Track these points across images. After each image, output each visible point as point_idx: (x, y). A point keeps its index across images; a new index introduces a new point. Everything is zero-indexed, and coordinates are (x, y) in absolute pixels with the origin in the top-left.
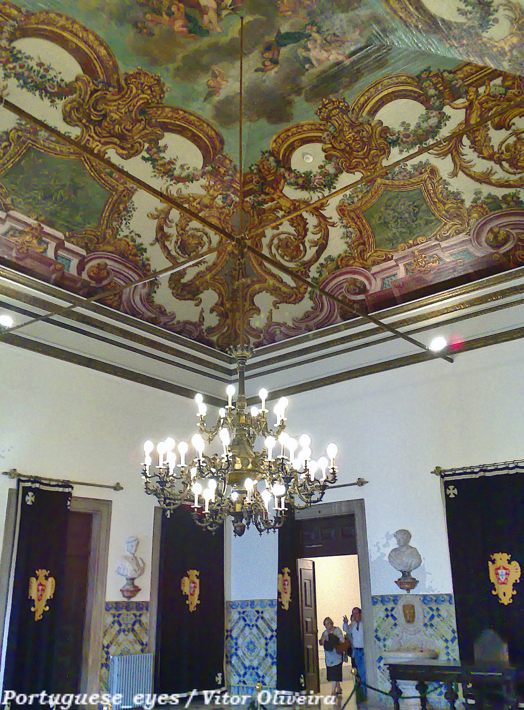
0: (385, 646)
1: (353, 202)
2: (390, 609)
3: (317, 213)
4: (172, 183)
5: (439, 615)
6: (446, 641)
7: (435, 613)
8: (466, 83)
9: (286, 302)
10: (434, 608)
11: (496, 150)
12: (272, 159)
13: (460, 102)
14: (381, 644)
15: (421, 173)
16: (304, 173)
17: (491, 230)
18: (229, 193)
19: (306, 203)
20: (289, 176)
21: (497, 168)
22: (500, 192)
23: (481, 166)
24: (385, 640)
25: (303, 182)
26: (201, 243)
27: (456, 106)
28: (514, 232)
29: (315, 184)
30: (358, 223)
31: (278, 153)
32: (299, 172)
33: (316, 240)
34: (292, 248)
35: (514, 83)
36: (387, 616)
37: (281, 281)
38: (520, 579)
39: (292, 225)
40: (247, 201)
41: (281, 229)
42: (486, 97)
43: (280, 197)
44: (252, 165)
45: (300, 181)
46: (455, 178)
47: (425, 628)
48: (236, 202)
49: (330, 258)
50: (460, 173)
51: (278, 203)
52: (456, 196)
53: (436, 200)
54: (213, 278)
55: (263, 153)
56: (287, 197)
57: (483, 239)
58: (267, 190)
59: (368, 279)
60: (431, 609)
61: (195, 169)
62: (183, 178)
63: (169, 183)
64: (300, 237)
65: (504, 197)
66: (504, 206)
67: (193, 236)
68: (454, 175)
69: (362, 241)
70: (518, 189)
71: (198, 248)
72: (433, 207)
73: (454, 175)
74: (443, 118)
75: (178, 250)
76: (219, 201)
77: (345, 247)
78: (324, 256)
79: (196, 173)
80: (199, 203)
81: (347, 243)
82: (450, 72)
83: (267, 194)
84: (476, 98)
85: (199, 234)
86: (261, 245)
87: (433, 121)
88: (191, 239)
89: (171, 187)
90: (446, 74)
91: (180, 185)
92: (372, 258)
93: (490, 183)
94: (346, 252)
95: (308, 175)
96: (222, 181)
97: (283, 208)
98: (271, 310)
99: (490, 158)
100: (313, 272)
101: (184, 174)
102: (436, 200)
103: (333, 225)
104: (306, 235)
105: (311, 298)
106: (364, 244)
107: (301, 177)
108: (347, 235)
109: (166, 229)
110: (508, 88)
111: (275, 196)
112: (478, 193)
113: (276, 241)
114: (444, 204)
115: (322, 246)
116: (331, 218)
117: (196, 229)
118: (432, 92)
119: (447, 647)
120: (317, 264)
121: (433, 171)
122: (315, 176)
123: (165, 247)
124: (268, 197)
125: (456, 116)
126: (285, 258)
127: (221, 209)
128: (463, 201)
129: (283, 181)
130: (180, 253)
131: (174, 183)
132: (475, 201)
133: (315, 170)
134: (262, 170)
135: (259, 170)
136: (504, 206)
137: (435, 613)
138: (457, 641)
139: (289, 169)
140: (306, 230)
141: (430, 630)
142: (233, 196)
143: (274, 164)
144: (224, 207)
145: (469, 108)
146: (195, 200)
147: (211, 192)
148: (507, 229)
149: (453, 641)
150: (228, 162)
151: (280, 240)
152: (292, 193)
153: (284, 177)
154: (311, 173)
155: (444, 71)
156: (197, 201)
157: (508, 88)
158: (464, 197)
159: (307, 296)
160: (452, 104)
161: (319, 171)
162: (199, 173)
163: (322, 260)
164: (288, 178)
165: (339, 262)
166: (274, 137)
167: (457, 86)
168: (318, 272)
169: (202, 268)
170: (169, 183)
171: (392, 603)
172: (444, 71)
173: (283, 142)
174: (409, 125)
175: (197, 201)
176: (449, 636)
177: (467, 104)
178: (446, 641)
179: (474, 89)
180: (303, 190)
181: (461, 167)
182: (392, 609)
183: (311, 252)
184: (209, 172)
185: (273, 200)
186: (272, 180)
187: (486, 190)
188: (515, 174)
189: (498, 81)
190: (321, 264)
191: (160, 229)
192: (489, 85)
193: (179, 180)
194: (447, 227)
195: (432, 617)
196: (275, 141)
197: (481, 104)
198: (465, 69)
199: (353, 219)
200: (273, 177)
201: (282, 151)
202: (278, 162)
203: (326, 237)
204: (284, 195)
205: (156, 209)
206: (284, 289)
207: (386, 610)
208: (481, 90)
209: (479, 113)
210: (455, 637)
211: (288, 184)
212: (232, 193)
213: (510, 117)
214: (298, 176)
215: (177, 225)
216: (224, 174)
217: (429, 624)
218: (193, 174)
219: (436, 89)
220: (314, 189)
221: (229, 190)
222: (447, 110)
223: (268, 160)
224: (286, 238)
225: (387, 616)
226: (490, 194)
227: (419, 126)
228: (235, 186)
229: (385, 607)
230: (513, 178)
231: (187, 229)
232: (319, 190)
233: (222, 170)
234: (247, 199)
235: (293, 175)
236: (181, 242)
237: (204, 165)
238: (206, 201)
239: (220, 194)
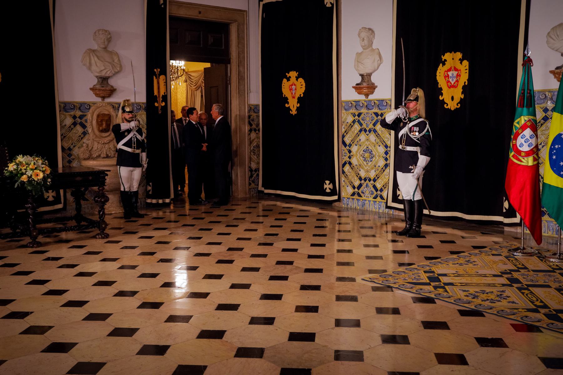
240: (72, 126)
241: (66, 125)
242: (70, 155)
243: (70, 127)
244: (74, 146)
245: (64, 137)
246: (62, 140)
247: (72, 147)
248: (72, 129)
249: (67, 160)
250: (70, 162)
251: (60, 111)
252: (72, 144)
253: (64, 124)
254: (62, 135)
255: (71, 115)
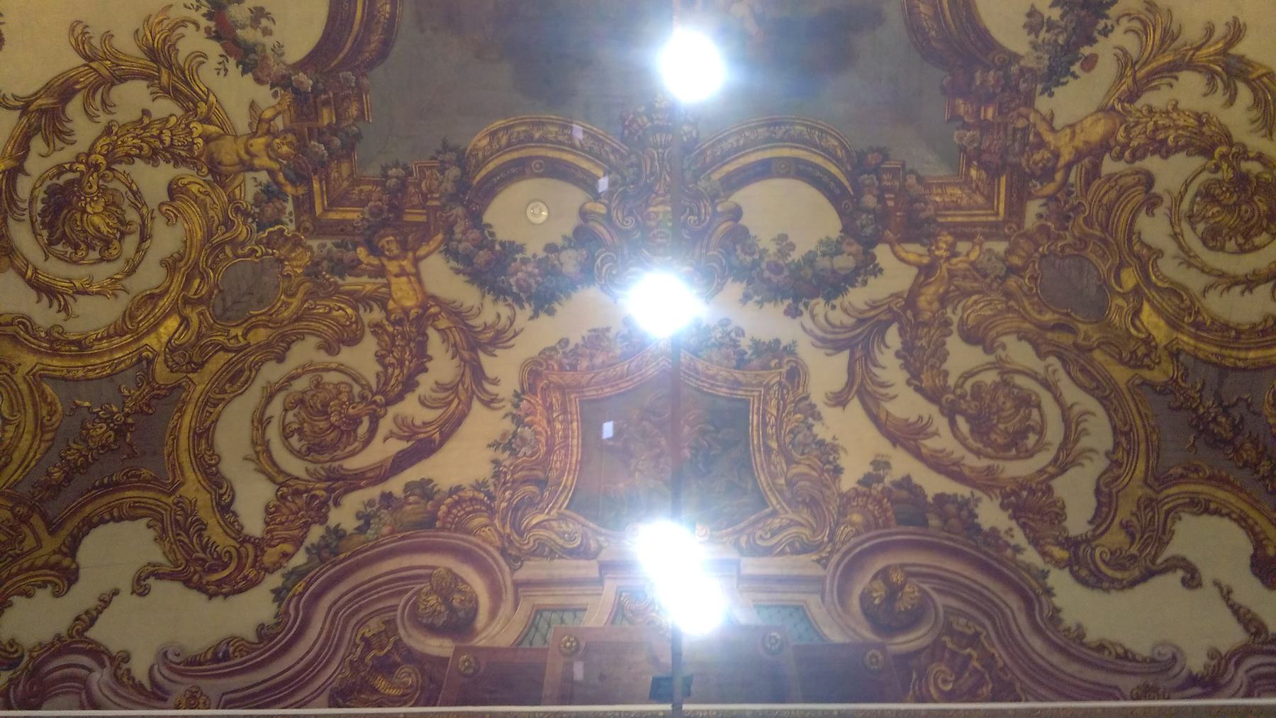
1: (574, 368)
3: (466, 355)
4: (204, 23)
8: (940, 220)
9: (187, 583)
11: (951, 381)
12: (454, 172)
13: (914, 251)
15: (766, 367)
16: (502, 244)
17: (884, 574)
18: (289, 189)
19: (458, 315)
20: (464, 233)
21: (941, 423)
22: (933, 484)
23: (907, 405)
25: (488, 263)
26: (107, 243)
27: (903, 255)
28: (940, 600)
29: (512, 281)
30: (558, 426)
31: (480, 165)
32: (492, 234)
33: (418, 422)
34: (333, 419)
35: (1024, 268)
37: (225, 508)
39: (380, 358)
40: (310, 248)
41: (347, 356)
42: (966, 265)
43: (403, 273)
44: (396, 165)
45: (482, 257)
46: (839, 409)
48: (282, 231)
49: (424, 489)
50: (855, 404)
51: (388, 285)
52: (827, 455)
53: (774, 445)
54: (37, 378)
55: (446, 148)
56: (420, 282)
57: (858, 590)
58: (383, 242)
59: (496, 593)
61: (278, 50)
62: (236, 42)
63: (197, 16)
64: (378, 398)
65: (941, 499)
66: (934, 522)
67: (112, 206)
68: (839, 400)
69: (540, 474)
70: (978, 493)
71: (90, 247)
72: (759, 459)
73: (839, 400)
74: (867, 268)
75: (41, 195)
76: (249, 187)
77: (484, 471)
78: (413, 474)
79: (271, 62)
80: (207, 139)
81: (496, 462)
82: (920, 180)
83: (374, 250)
84: (948, 259)
85: (132, 215)
86: (249, 381)
87: (844, 262)
88: (99, 208)
89: (191, 26)
90: (912, 180)
91: (214, 49)
92: (542, 533)
93: (918, 455)
94: (480, 486)
95: (512, 249)
96: (301, 147)
97: (391, 305)
98: (116, 593)
99: (933, 396)
100: (344, 516)
101: (248, 35)
102: (774, 445)
103: (490, 402)
104: (400, 397)
105: (278, 594)
106: (542, 483)
107: (492, 248)
108: (508, 444)
109: (74, 107)
110: (1012, 270)
111: (393, 267)
112: (881, 464)
113: (301, 384)
114: (790, 461)
115: (422, 447)
116: (495, 382)
117: (136, 194)
118: (870, 201)
120: (374, 492)
121: (796, 375)
122: (525, 261)
123: (23, 145)
124: (375, 262)
125: (894, 272)
126: (295, 441)
127: (237, 210)
128: (838, 471)
129: (440, 237)
130: (39, 206)
131: (208, 30)
132: (867, 481)
133: (535, 248)
134: (412, 189)
135: (403, 184)
136: (934, 522)
139: (475, 218)
140: (409, 385)
142: (290, 207)
143: (449, 186)
144: (246, 214)
145: (926, 271)
146: (207, 120)
147: (259, 143)
148: (926, 587)
150: (353, 111)
151: (318, 385)
152: (441, 276)
153: (450, 231)
154: (521, 249)
155: (912, 172)
156: (212, 129)
157: (1012, 270)
158: (844, 461)
159: (275, 580)
160: (898, 248)
161: (541, 254)
162: (277, 69)
163: (396, 485)
164: (458, 236)
165: (444, 508)
166: (500, 123)
167: (923, 215)
168: (359, 516)
169: (43, 315)
170: (197, 16)
172: (912, 172)
173: (509, 144)
174: (792, 247)
175: (212, 129)
177: (926, 260)
179: (950, 239)
180: (471, 282)
181: (861, 389)
183: (382, 449)
184: (296, 91)
185: (381, 272)
186: (417, 224)
187: (903, 465)
188: (978, 453)
189: (1000, 247)
190: (387, 498)
191: (64, 90)
192: (981, 245)
193: (223, 33)
194: (777, 523)
196: (493, 134)
197: (952, 275)
198: (950, 190)
199: (549, 408)
200: (423, 219)
201: (491, 166)
202: (463, 185)
203: (449, 428)
204: (418, 275)
205: (108, 36)
206: (216, 534)
208: (963, 247)
209: (941, 290)
211: (447, 251)
212: (296, 199)
213: (999, 329)
214: (486, 241)
215: (108, 131)
216: (321, 133)
218: (265, 57)
219: (881, 199)
220: (500, 292)
221: (293, 183)
222: (883, 253)
223: (442, 172)
224: (336, 386)
226: (908, 479)
227: (810, 259)
228: (316, 186)
230: (972, 461)
231: (119, 168)
232: (510, 300)
233: (327, 117)
234: (315, 243)
235: (474, 234)
236: (71, 183)
237: (302, 65)
238: (228, 152)
239: (271, 172)
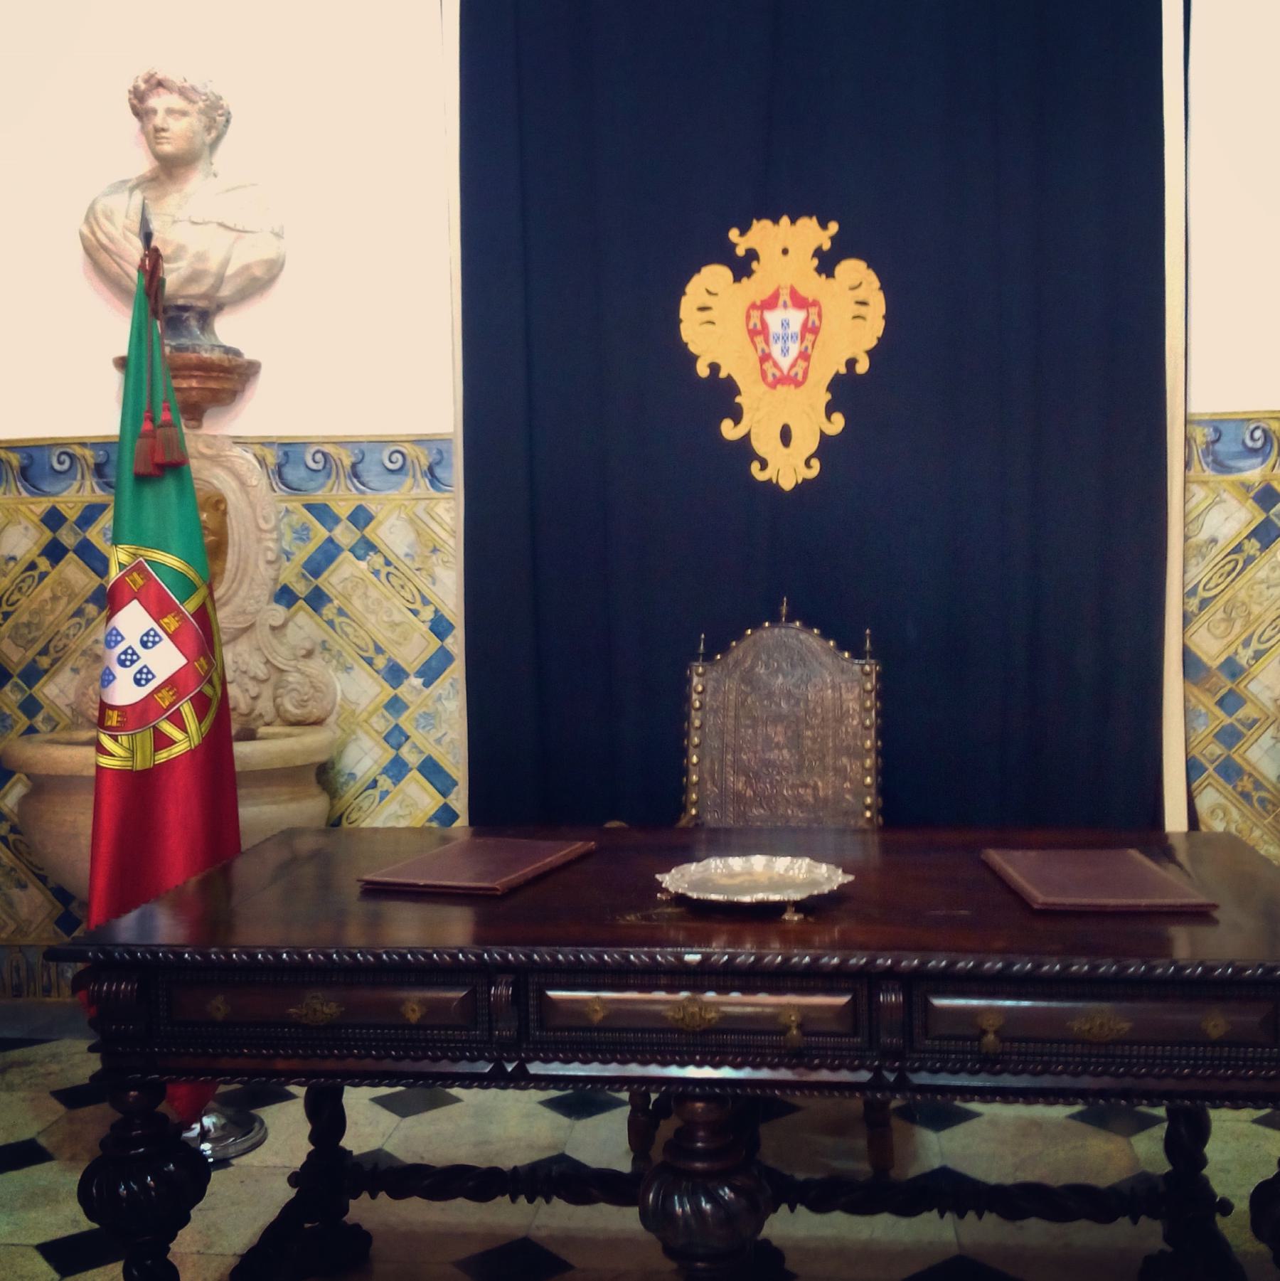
0: (31, 706)
2: (72, 514)
5: (366, 547)
6: (395, 674)
7: (345, 535)
10: (343, 510)
14: (11, 696)
24: (32, 675)
36: (54, 552)
38: (871, 353)
47: (278, 613)
60: (322, 512)
119: (395, 705)
137: (345, 535)
138: (457, 670)
141: (304, 625)
149: (430, 673)
171: (90, 482)
176: (415, 648)
178: (395, 674)
182: (90, 515)
195: (327, 555)
207: (53, 519)
210: (444, 658)
217: (301, 588)
225: (54, 552)
229: (41, 506)
240: (1252, 547)
241: (1214, 541)
242: (1230, 702)
243: (1238, 549)
244: (1258, 655)
245: (1204, 603)
246: (1187, 619)
247: (1244, 657)
248: (1249, 560)
249: (1214, 726)
250: (1229, 736)
251: (1187, 465)
252: (1246, 644)
253: (1203, 536)
254: (1189, 594)
255: (1247, 487)
